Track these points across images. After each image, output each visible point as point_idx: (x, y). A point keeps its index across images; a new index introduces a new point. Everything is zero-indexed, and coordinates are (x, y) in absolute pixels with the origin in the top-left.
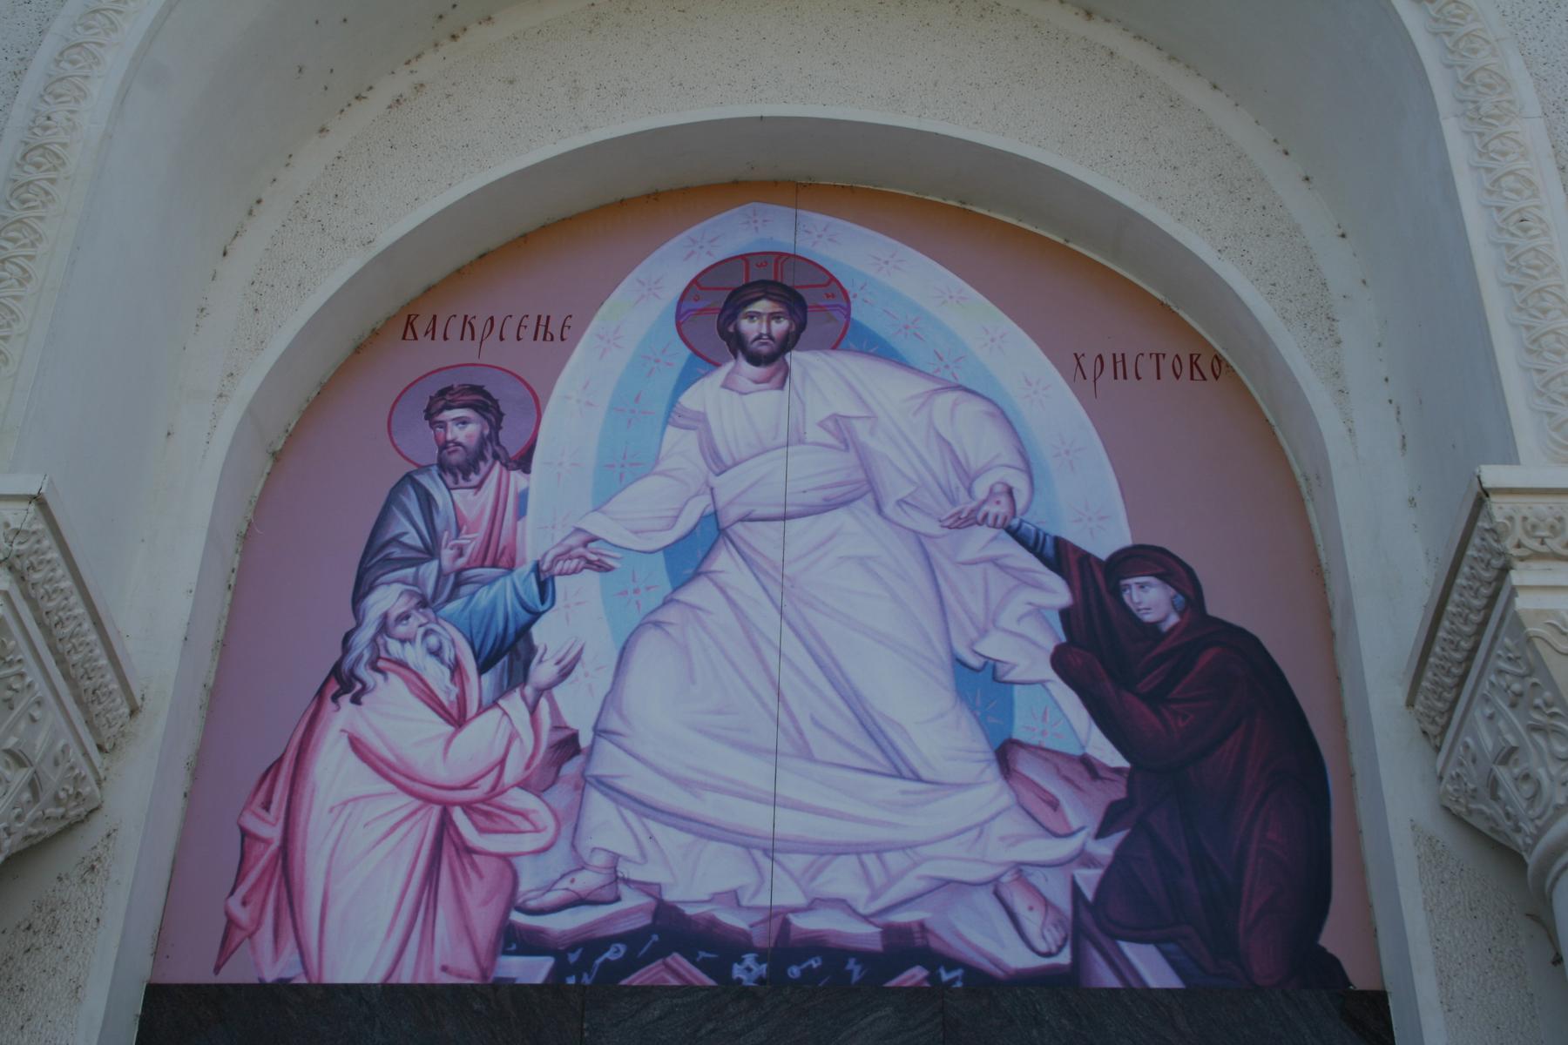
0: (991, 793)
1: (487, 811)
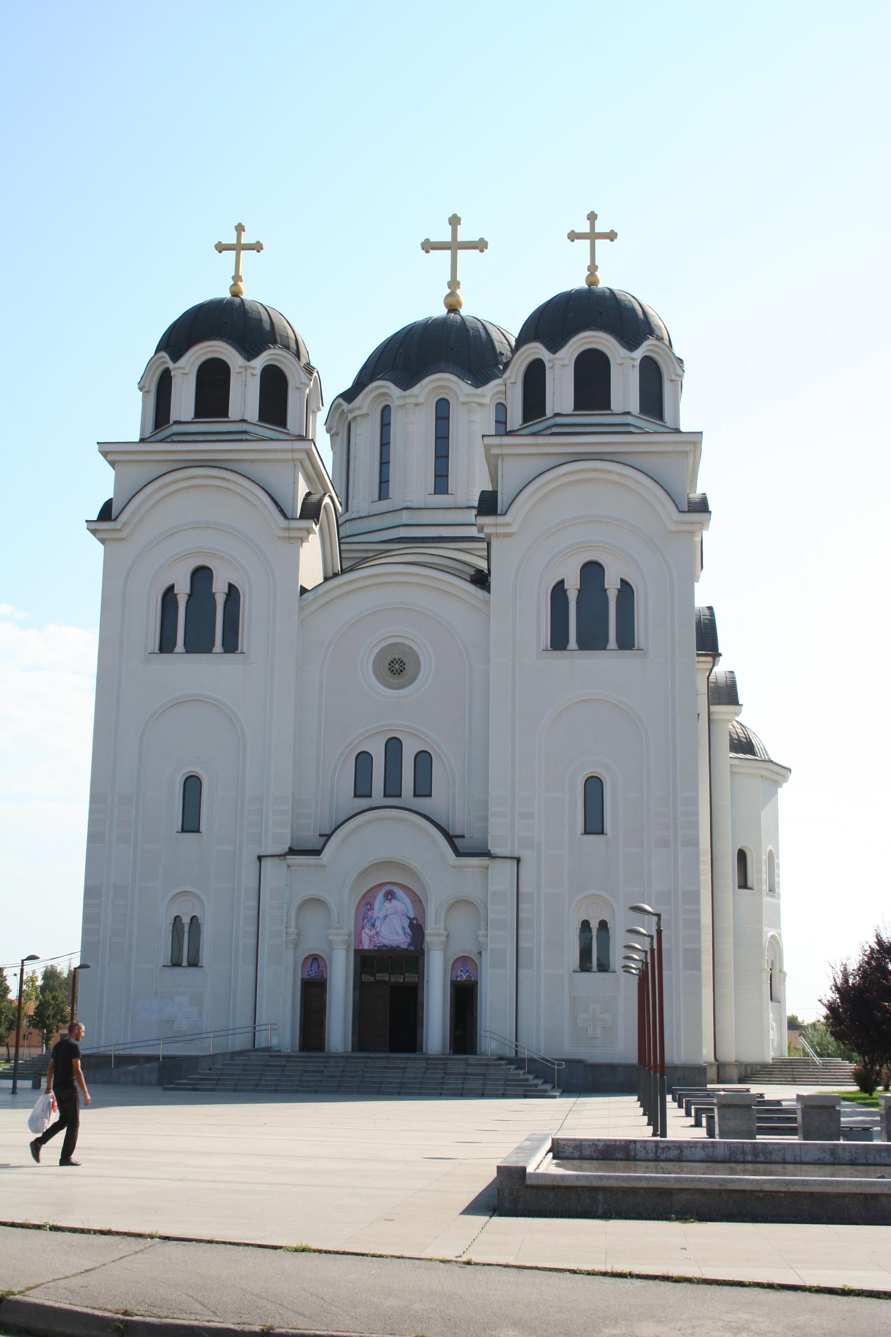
0: (403, 936)
1: (373, 937)
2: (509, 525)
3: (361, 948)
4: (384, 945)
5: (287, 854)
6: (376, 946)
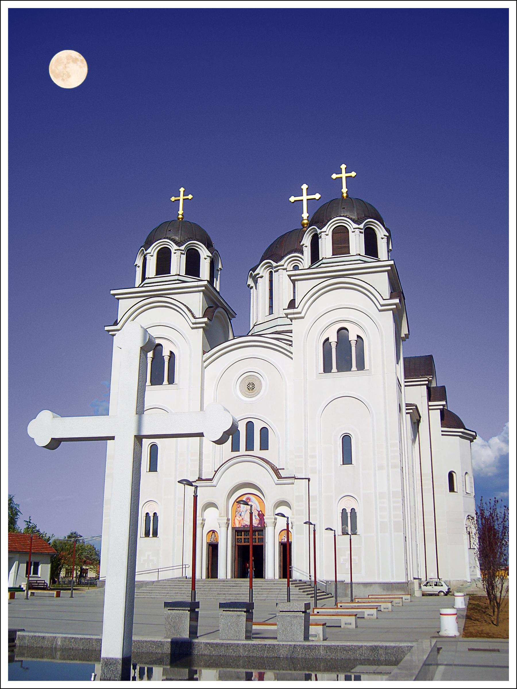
1: (241, 521)
2: (300, 313)
3: (235, 527)
4: (246, 525)
5: (197, 480)
6: (242, 525)
